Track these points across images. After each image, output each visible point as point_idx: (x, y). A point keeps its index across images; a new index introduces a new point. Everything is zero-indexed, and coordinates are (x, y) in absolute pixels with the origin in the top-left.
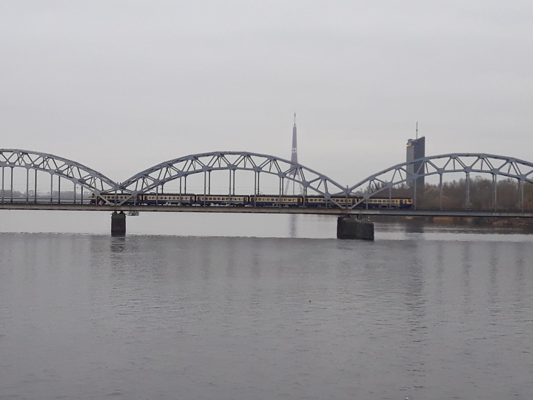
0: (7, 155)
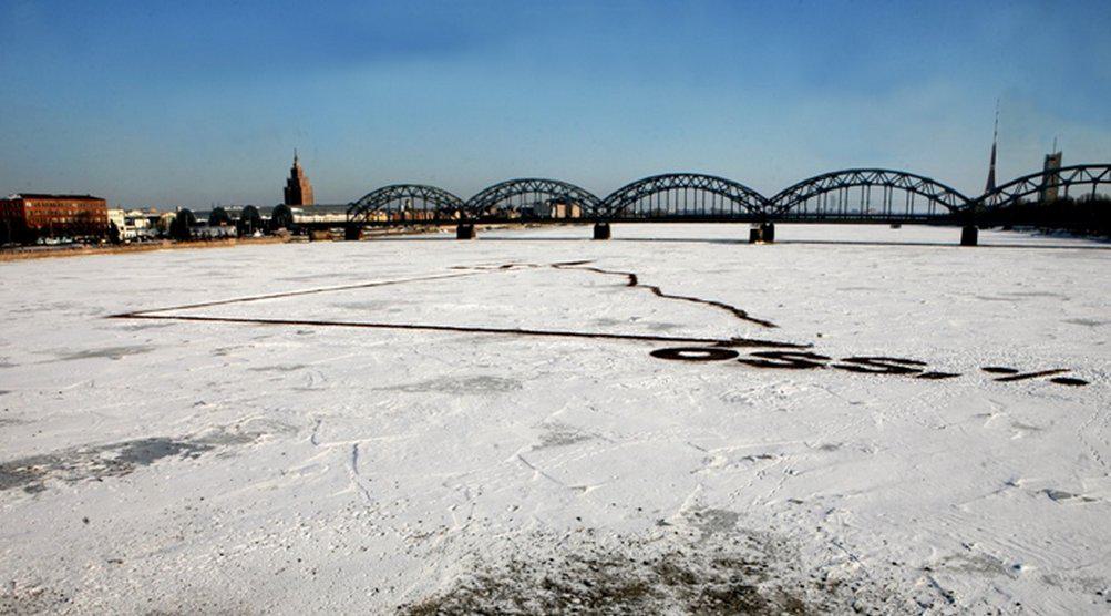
0: (866, 175)
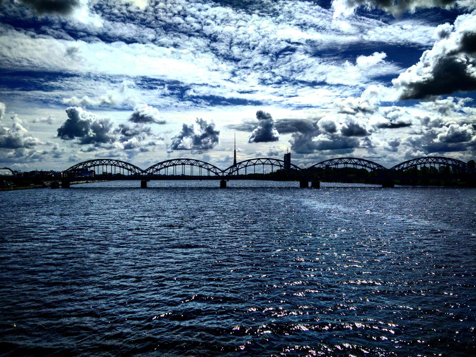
0: (105, 161)
